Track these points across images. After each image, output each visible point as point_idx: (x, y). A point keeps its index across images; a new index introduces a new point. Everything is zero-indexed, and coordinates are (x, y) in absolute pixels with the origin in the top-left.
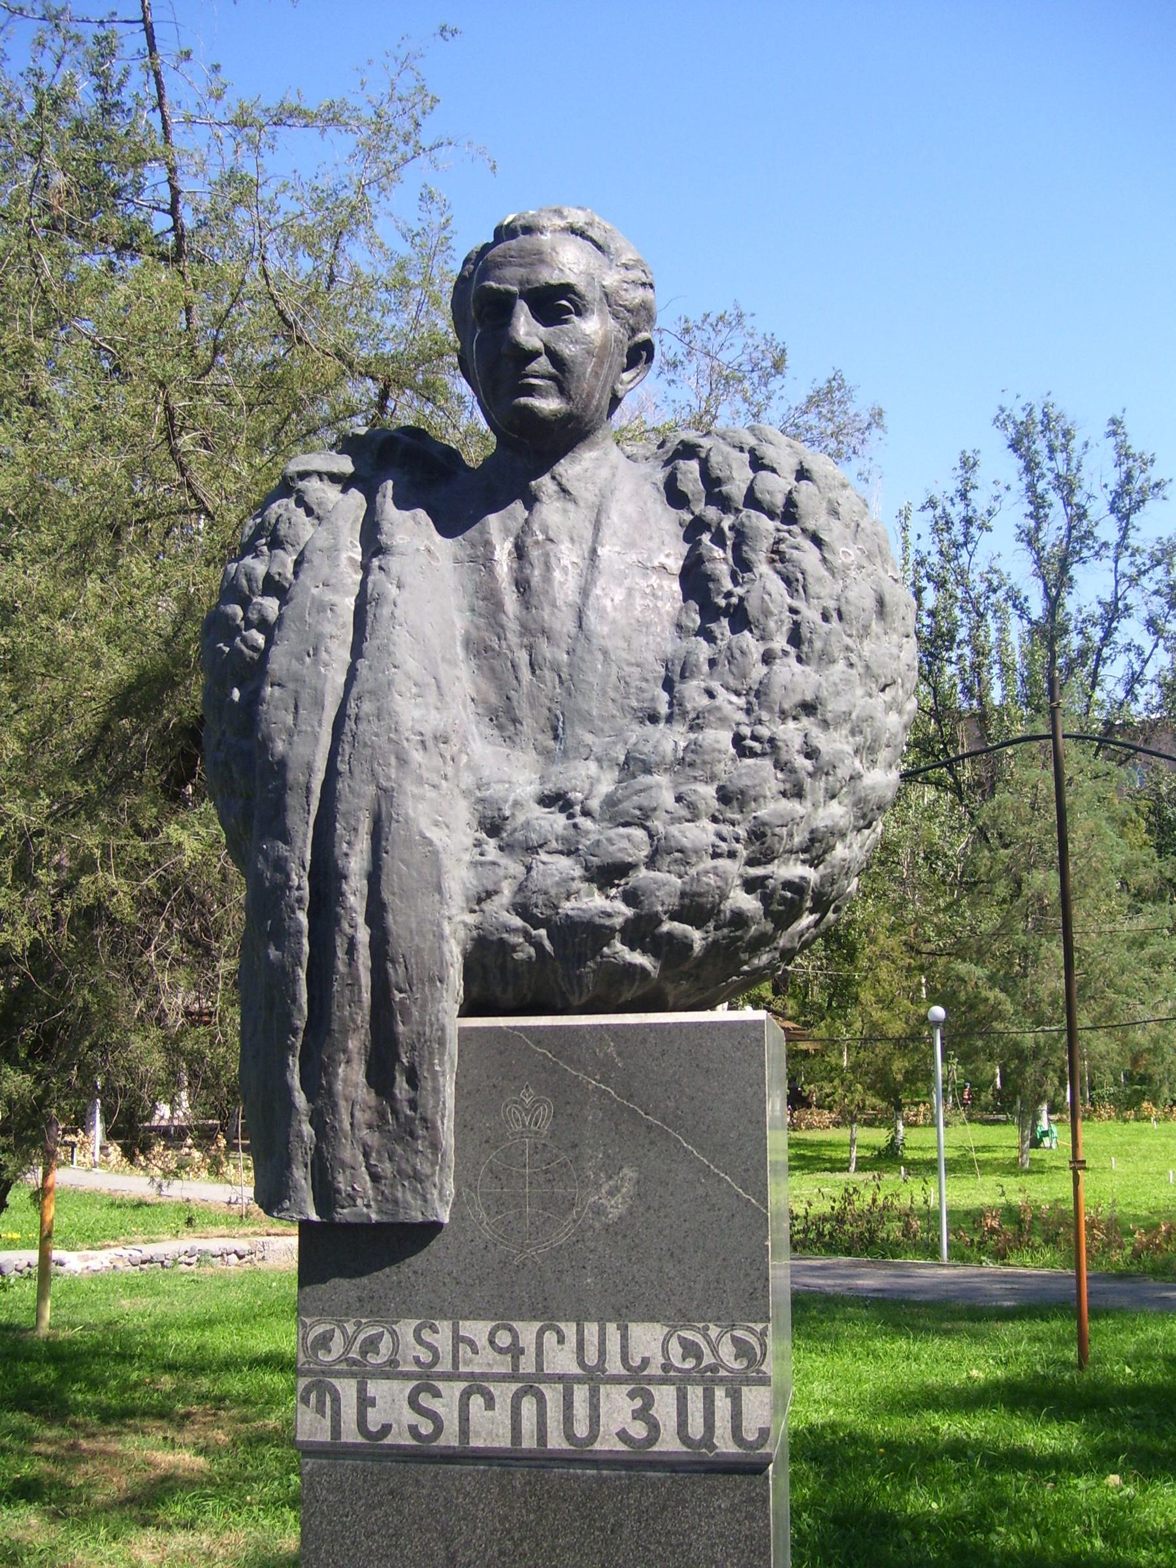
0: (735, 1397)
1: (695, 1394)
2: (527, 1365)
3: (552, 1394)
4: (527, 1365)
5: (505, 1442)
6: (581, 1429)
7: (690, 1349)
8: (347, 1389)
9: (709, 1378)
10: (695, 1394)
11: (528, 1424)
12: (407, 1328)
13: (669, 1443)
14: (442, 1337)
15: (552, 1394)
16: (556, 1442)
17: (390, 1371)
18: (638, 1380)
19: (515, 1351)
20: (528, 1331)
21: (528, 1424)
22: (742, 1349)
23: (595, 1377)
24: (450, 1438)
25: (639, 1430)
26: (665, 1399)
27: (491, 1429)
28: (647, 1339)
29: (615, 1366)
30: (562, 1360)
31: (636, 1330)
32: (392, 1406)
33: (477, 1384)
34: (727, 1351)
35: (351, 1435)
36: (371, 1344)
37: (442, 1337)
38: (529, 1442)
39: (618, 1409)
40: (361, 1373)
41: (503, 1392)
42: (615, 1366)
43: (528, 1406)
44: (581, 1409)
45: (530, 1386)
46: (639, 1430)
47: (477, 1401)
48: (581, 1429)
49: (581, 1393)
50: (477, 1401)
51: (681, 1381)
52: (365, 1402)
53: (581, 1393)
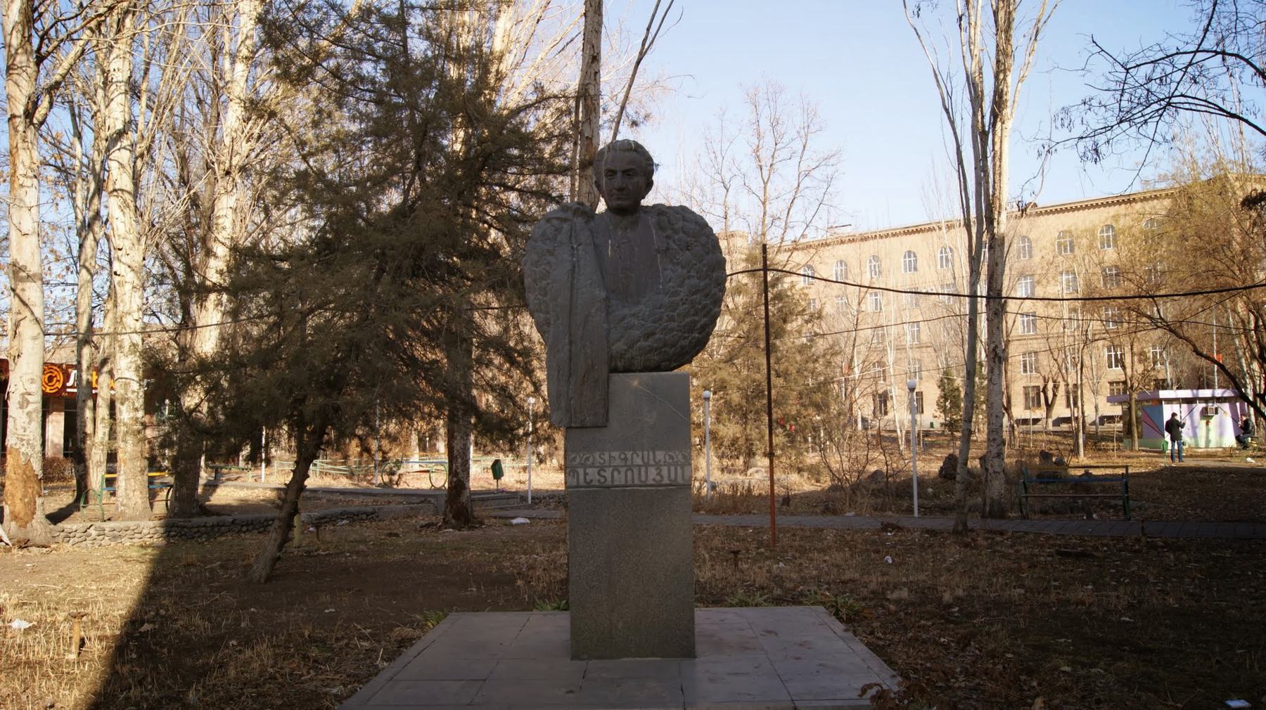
0: (682, 468)
1: (672, 468)
2: (629, 463)
3: (636, 470)
4: (629, 463)
5: (623, 482)
6: (643, 478)
7: (671, 457)
8: (581, 471)
9: (676, 465)
10: (672, 468)
11: (629, 478)
12: (597, 455)
13: (666, 481)
14: (606, 456)
15: (636, 470)
16: (636, 482)
17: (592, 466)
18: (658, 466)
19: (626, 459)
20: (629, 454)
21: (629, 478)
22: (684, 457)
23: (647, 465)
24: (609, 482)
25: (658, 478)
26: (665, 471)
27: (619, 479)
28: (660, 455)
29: (652, 462)
30: (638, 461)
31: (657, 453)
32: (592, 473)
33: (616, 468)
34: (680, 457)
35: (582, 482)
36: (587, 459)
37: (606, 456)
38: (630, 483)
39: (653, 472)
40: (584, 466)
41: (623, 470)
42: (652, 462)
43: (629, 474)
44: (643, 474)
45: (630, 468)
46: (658, 478)
47: (616, 473)
48: (643, 478)
49: (643, 469)
50: (616, 473)
51: (669, 465)
52: (586, 474)
53: (643, 469)
